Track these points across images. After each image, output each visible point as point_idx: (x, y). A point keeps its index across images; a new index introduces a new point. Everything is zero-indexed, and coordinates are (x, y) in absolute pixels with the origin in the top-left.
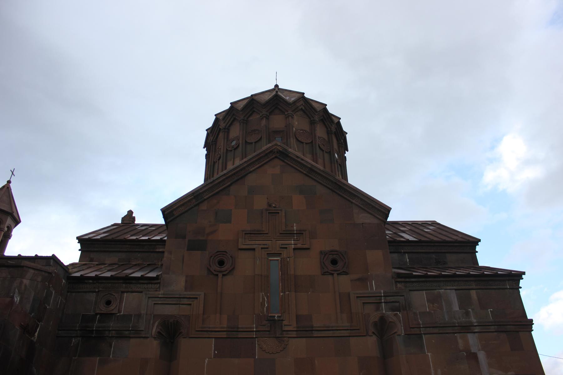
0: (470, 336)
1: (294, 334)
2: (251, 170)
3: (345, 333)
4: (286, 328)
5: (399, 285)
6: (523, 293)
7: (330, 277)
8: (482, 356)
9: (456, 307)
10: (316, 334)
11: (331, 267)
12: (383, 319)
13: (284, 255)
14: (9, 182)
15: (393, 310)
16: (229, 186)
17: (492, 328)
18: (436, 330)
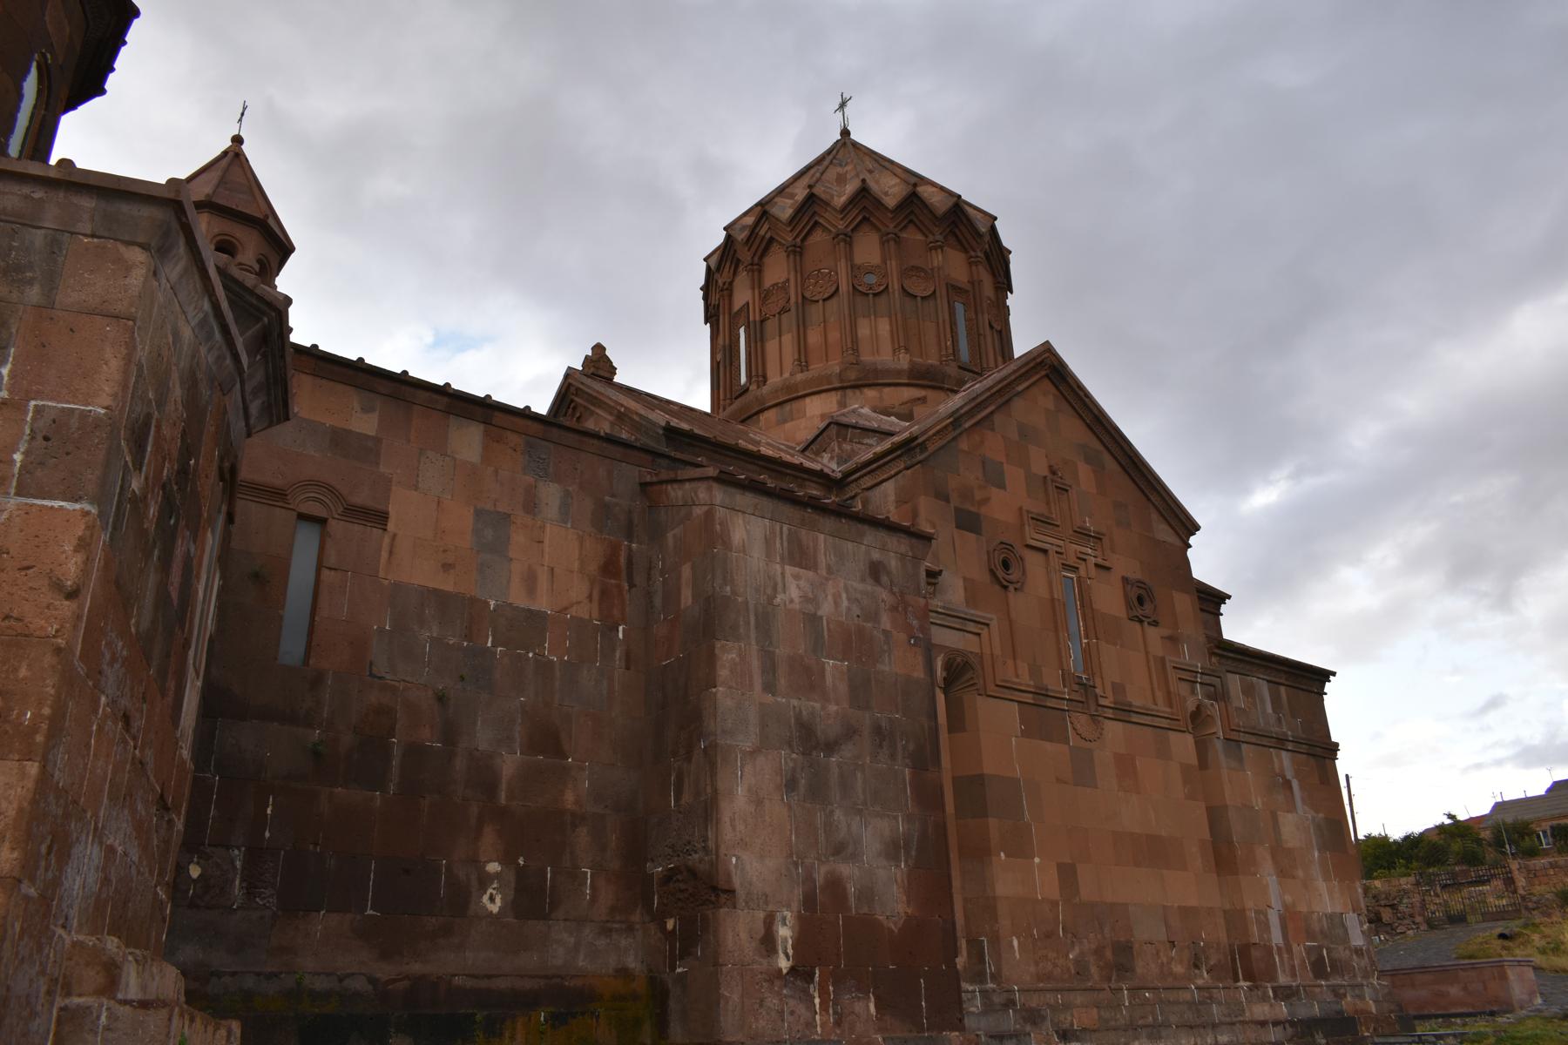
0: (1284, 754)
1: (1109, 713)
2: (1020, 388)
3: (1164, 723)
4: (1102, 702)
5: (1214, 659)
6: (1328, 701)
7: (1137, 626)
8: (1295, 784)
9: (1270, 710)
10: (1135, 718)
11: (1139, 612)
12: (1198, 707)
13: (1082, 572)
14: (238, 140)
15: (1209, 698)
16: (992, 413)
17: (1304, 748)
18: (1253, 739)
